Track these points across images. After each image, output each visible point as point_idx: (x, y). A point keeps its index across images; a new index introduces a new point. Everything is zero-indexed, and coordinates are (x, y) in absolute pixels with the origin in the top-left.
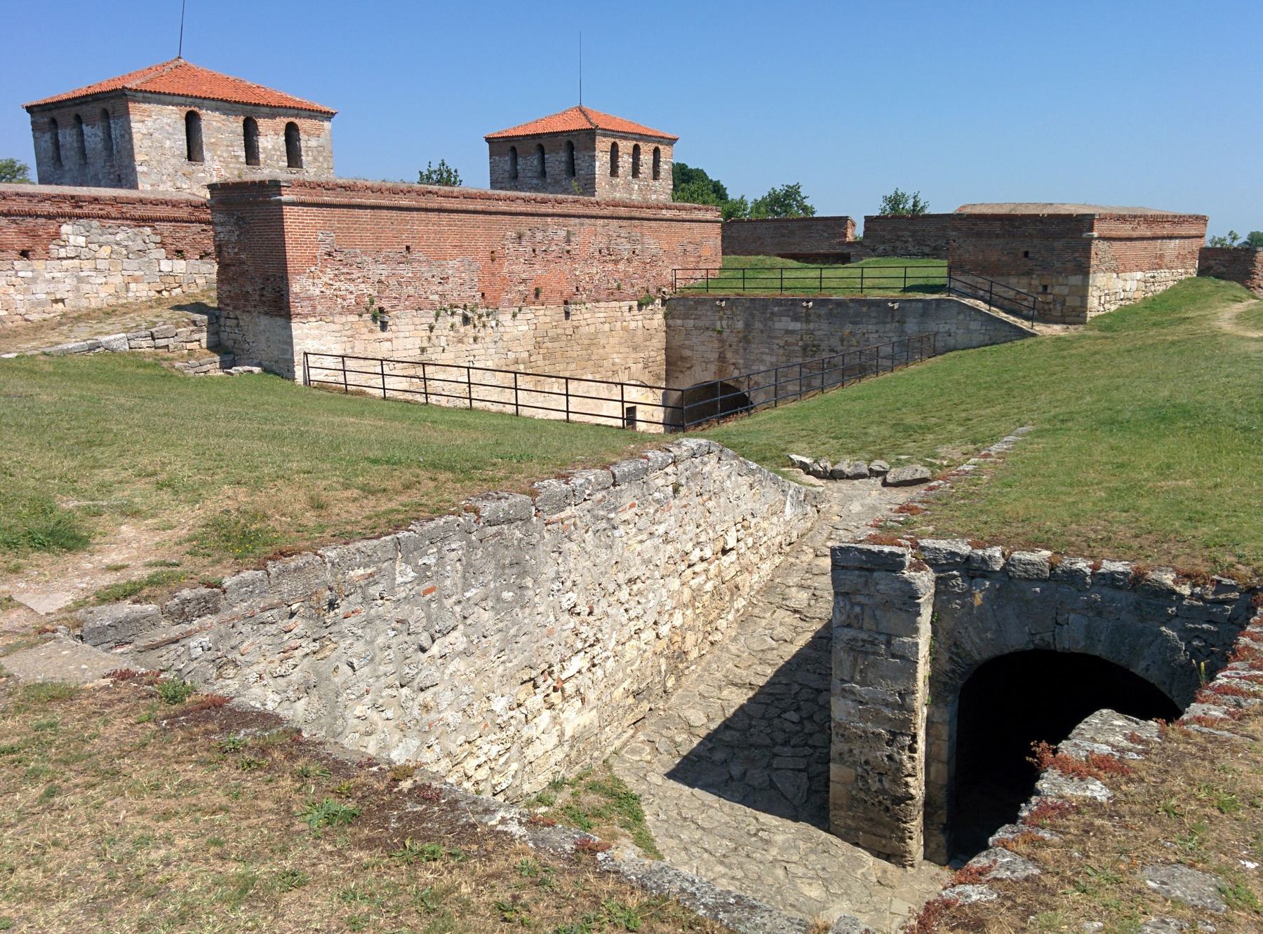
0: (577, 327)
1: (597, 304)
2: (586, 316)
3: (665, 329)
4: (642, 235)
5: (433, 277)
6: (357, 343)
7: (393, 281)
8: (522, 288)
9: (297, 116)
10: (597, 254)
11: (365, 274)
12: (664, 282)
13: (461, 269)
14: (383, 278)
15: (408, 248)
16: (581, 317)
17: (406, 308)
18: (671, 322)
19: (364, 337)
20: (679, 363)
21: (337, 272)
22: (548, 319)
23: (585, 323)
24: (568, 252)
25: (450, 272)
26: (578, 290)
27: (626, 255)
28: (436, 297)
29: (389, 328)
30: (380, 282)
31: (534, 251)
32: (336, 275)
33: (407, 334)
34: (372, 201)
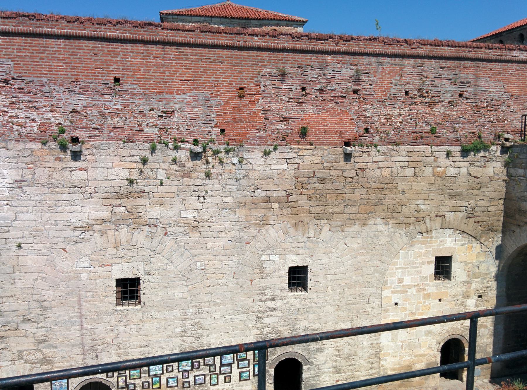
0: (362, 170)
1: (395, 148)
2: (376, 159)
3: (506, 178)
4: (477, 77)
5: (152, 110)
6: (38, 170)
7: (93, 112)
8: (281, 126)
9: (277, 25)
10: (402, 96)
11: (54, 102)
12: (508, 128)
13: (194, 104)
14: (79, 109)
15: (117, 80)
16: (370, 159)
17: (110, 139)
18: (512, 171)
19: (49, 165)
20: (517, 216)
21: (14, 100)
22: (318, 160)
23: (375, 165)
24: (355, 92)
25: (177, 106)
26: (367, 130)
27: (448, 97)
28: (155, 131)
29: (83, 158)
30: (74, 111)
31: (303, 89)
32: (13, 103)
33: (110, 165)
34: (67, 31)
